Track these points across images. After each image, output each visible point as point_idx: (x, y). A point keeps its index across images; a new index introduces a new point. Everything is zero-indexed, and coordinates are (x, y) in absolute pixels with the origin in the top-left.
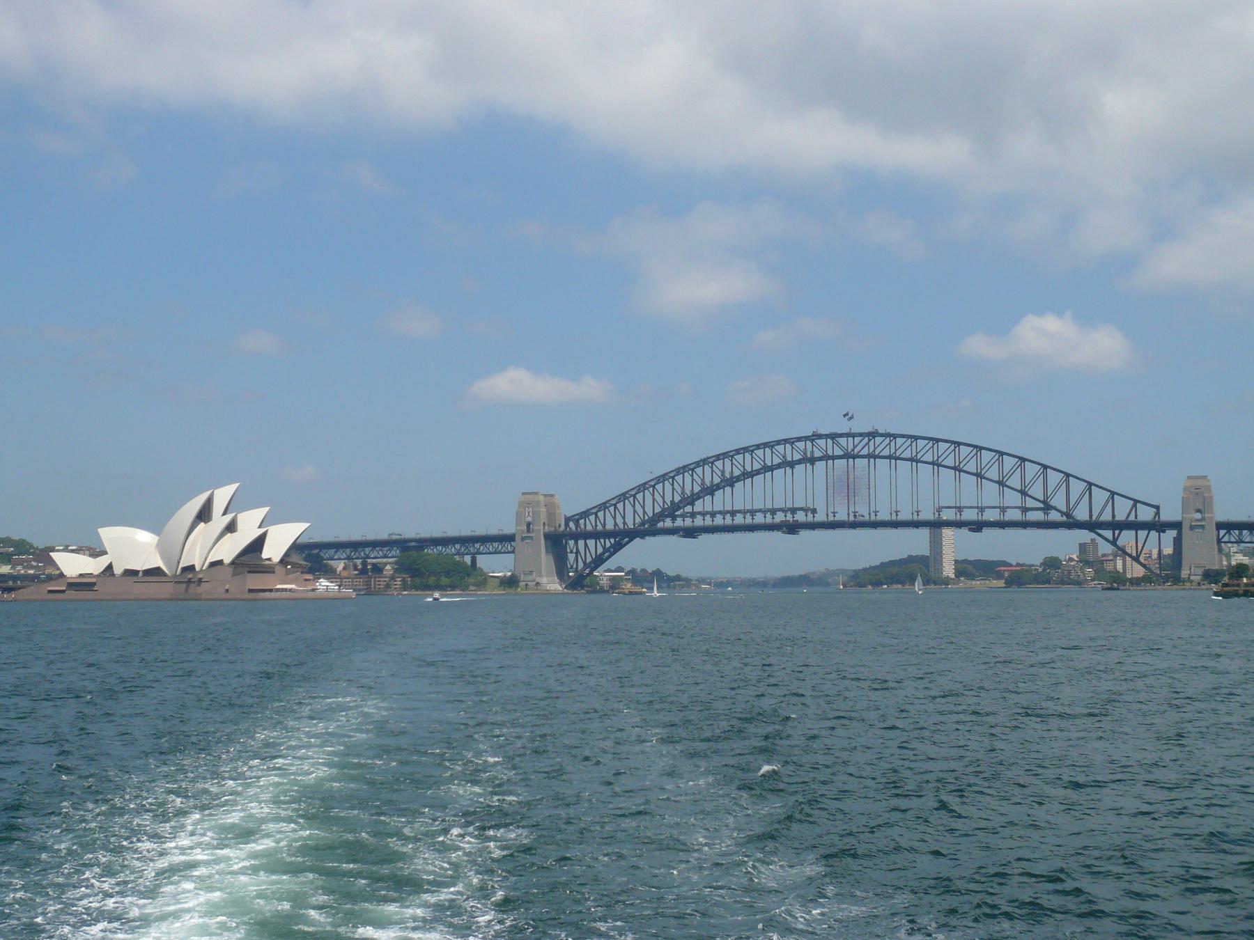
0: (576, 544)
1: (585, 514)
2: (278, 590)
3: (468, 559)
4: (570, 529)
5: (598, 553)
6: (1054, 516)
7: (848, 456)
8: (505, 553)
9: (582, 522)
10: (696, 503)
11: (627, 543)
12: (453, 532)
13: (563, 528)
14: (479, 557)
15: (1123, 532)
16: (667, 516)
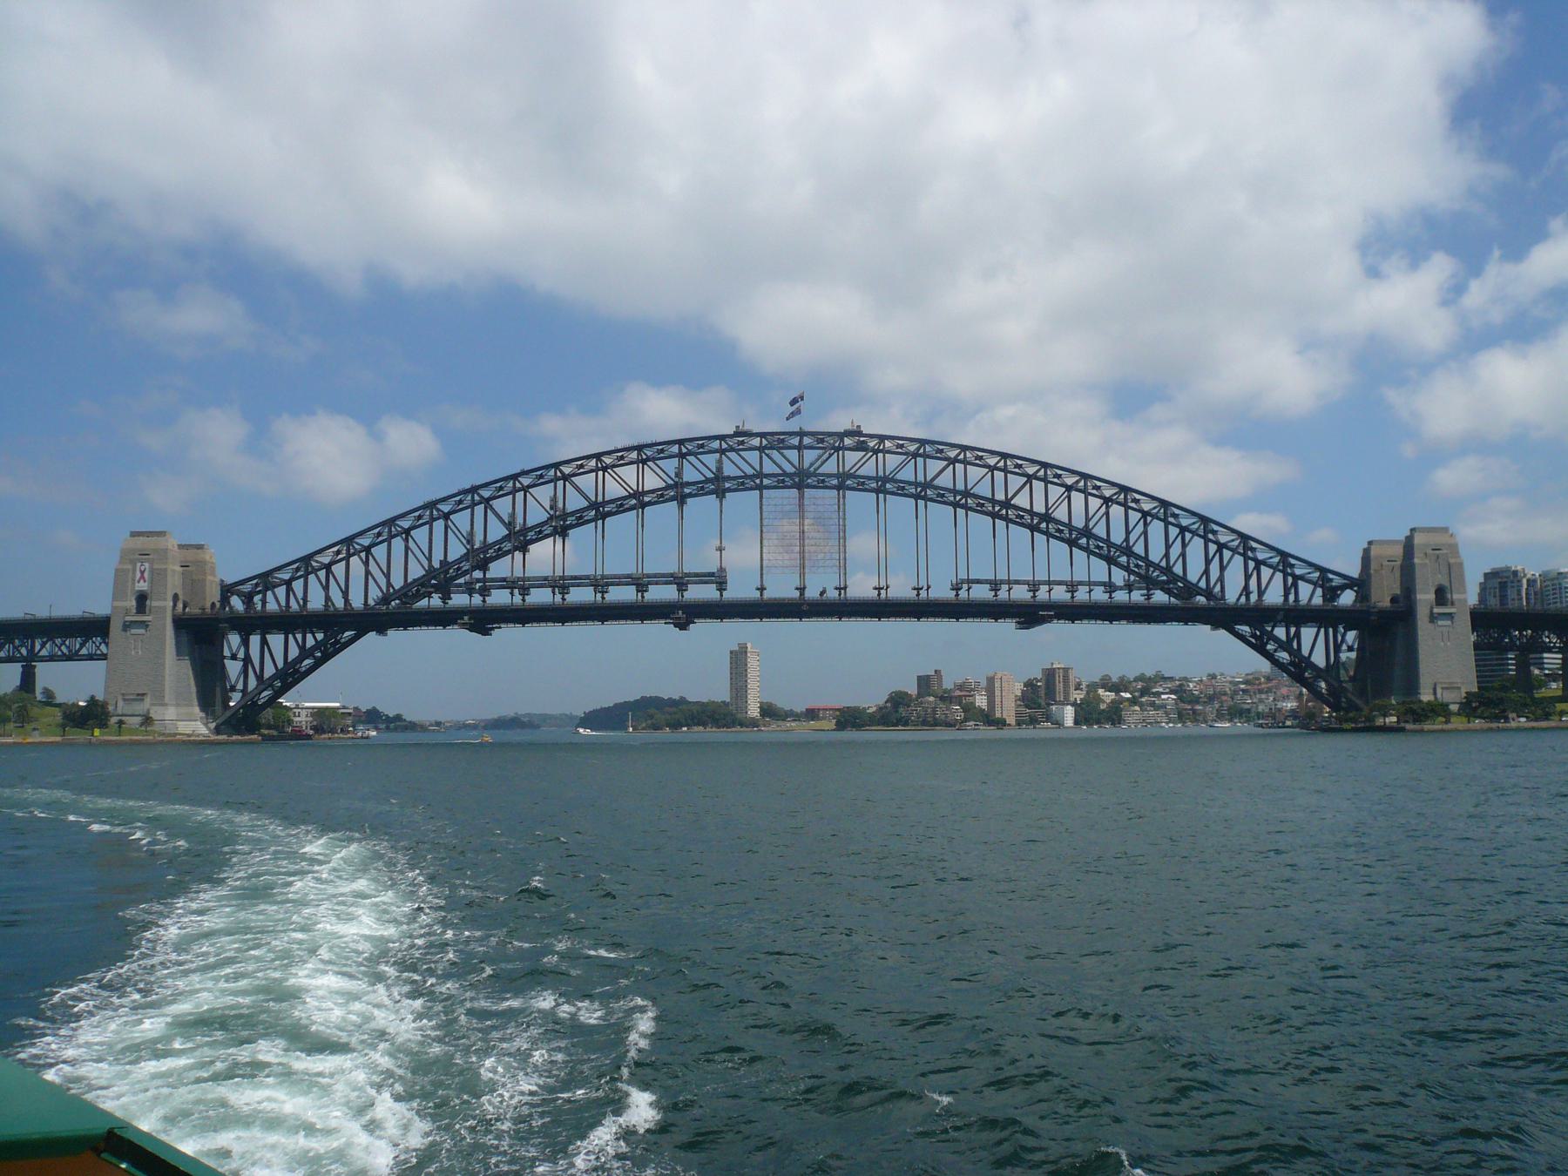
1: (266, 581)
4: (231, 608)
9: (257, 598)
10: (492, 566)
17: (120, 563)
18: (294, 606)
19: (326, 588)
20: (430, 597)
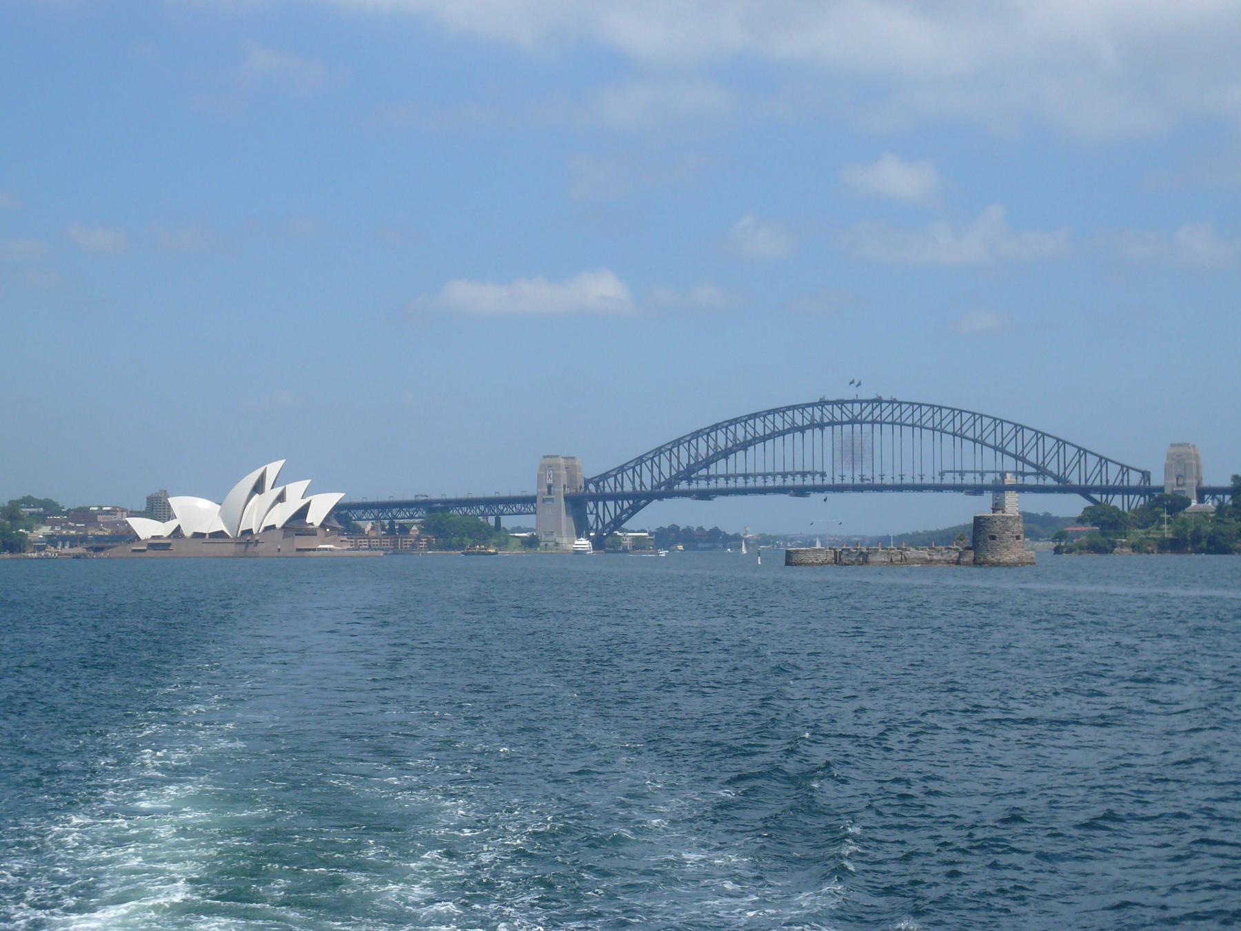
1: (604, 477)
2: (320, 549)
3: (492, 521)
6: (1050, 481)
7: (852, 422)
8: (528, 513)
11: (645, 505)
12: (477, 494)
13: (583, 490)
14: (502, 518)
17: (540, 470)
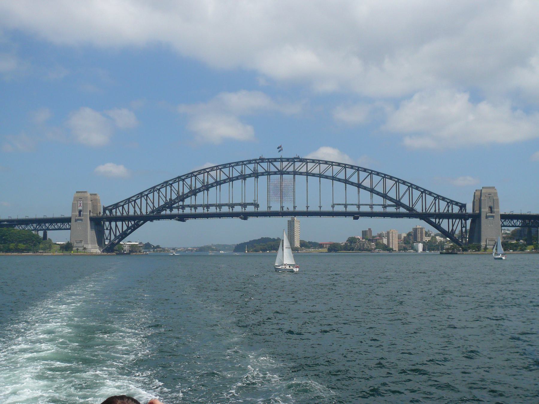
0: (110, 224)
1: (116, 206)
3: (41, 234)
4: (106, 214)
5: (124, 230)
8: (65, 229)
9: (114, 211)
10: (185, 200)
12: (32, 216)
13: (102, 213)
15: (444, 220)
16: (168, 208)
17: (74, 201)
18: (125, 214)
19: (134, 208)
20: (166, 211)
